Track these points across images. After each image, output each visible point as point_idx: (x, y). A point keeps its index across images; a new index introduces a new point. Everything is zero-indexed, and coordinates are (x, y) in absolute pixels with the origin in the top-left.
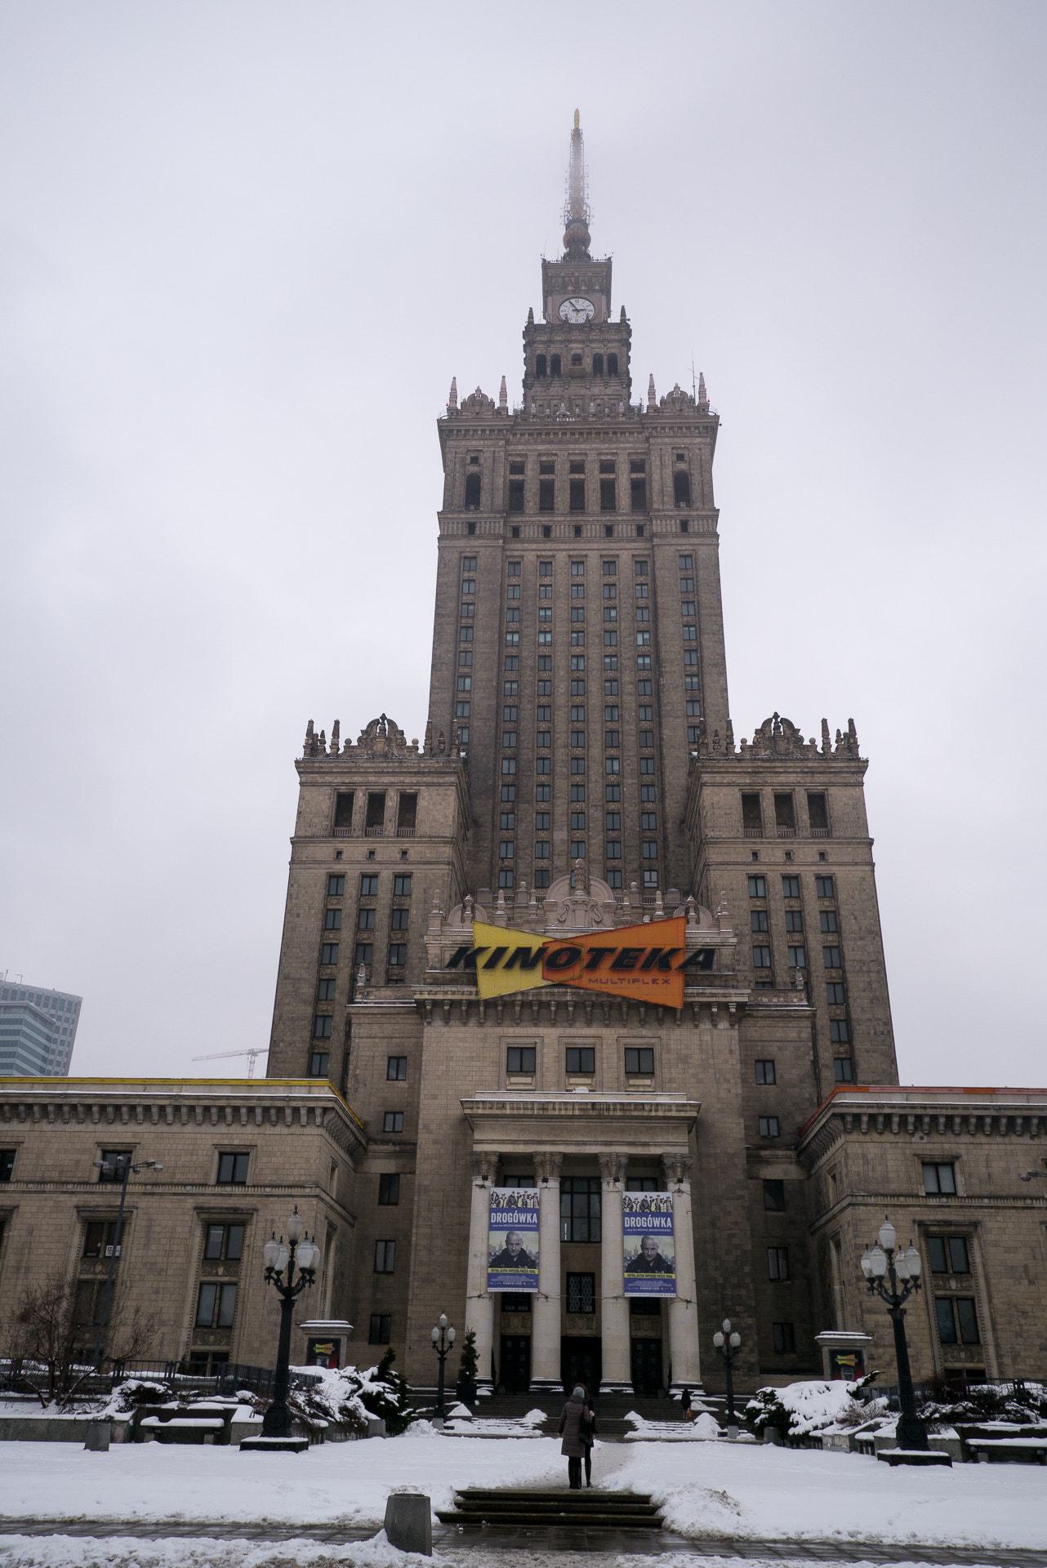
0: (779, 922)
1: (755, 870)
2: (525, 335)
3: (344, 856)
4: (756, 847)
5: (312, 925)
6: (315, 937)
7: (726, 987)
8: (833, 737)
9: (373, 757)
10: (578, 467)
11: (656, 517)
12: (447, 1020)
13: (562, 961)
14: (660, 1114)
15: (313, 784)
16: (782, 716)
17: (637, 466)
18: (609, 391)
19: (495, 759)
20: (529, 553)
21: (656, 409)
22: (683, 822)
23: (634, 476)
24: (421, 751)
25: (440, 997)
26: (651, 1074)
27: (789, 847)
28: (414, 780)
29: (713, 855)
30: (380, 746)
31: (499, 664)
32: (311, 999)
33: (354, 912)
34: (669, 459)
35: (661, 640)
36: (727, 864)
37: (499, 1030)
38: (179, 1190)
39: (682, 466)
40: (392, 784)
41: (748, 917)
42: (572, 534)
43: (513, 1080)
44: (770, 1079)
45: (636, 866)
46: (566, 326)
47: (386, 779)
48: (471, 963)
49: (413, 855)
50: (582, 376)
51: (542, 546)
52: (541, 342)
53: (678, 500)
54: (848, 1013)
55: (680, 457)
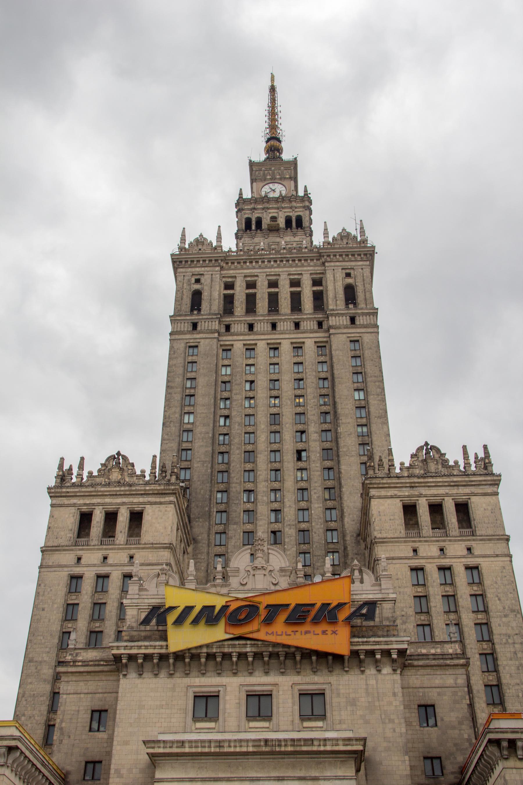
0: (437, 604)
1: (415, 563)
2: (237, 205)
3: (83, 561)
4: (416, 545)
6: (56, 627)
7: (388, 636)
8: (472, 460)
11: (332, 315)
13: (242, 617)
14: (328, 748)
15: (61, 506)
16: (431, 443)
17: (317, 282)
19: (211, 491)
21: (329, 243)
22: (358, 535)
23: (315, 288)
24: (147, 478)
25: (134, 651)
26: (323, 717)
27: (442, 544)
28: (141, 500)
30: (115, 476)
31: (214, 421)
32: (50, 678)
33: (89, 605)
35: (337, 400)
37: (187, 681)
39: (349, 281)
40: (124, 504)
41: (411, 601)
42: (270, 328)
44: (431, 722)
46: (266, 199)
51: (247, 337)
52: (248, 209)
53: (347, 304)
54: (499, 679)
55: (348, 275)
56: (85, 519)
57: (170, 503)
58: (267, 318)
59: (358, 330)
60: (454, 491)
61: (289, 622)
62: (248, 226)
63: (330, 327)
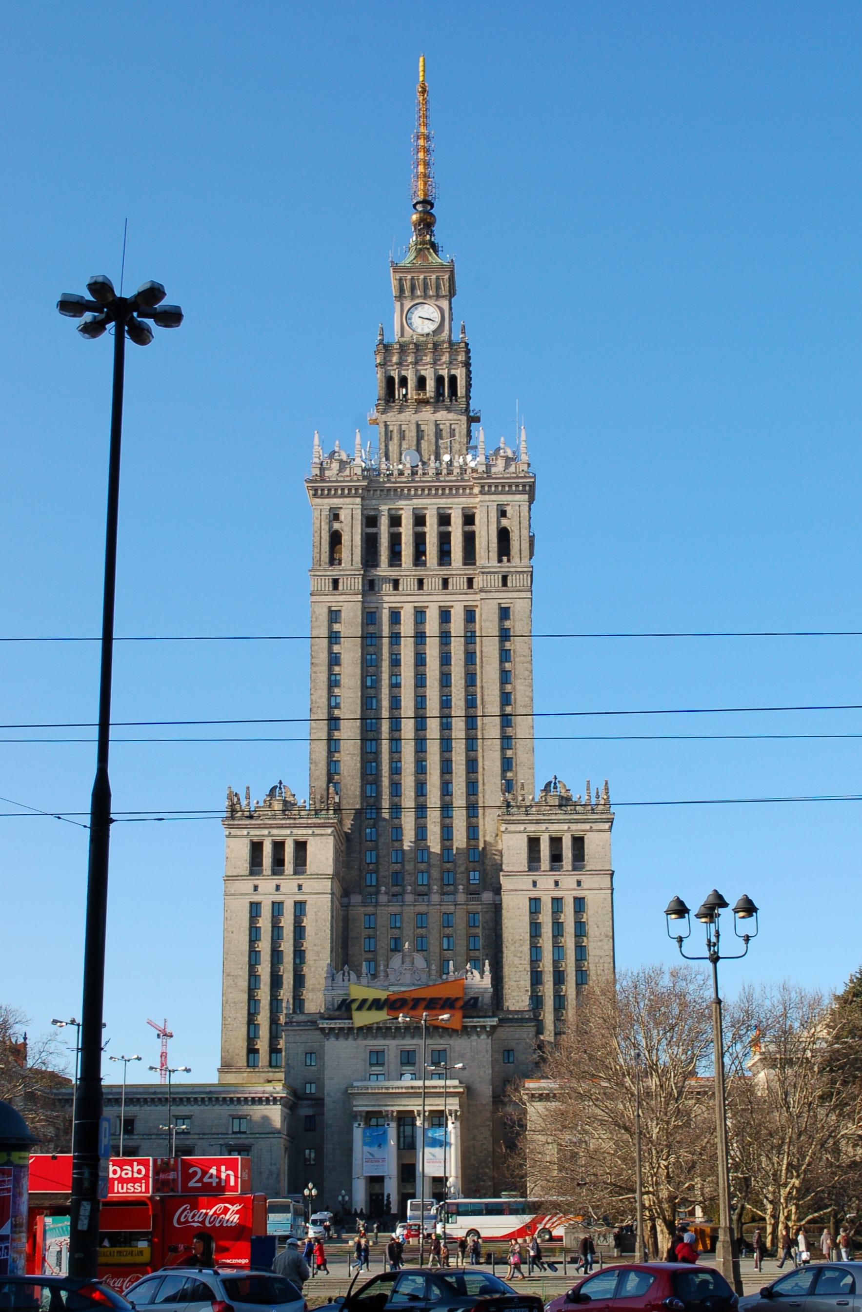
1: (534, 894)
3: (259, 889)
12: (337, 1037)
17: (469, 519)
27: (557, 878)
29: (506, 883)
32: (246, 989)
34: (493, 515)
35: (484, 685)
36: (516, 890)
37: (365, 1042)
38: (215, 1136)
43: (373, 1068)
44: (511, 1059)
49: (305, 888)
50: (426, 402)
57: (329, 835)
58: (413, 573)
59: (511, 595)
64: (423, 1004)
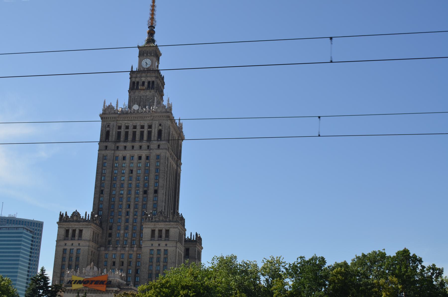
0: (155, 260)
1: (151, 248)
5: (60, 260)
6: (60, 263)
9: (73, 221)
10: (135, 127)
12: (67, 292)
17: (150, 127)
18: (151, 94)
20: (120, 154)
23: (149, 130)
27: (159, 243)
30: (75, 218)
33: (68, 258)
34: (157, 126)
39: (160, 128)
40: (77, 228)
41: (148, 259)
45: (138, 240)
47: (76, 226)
48: (71, 283)
51: (124, 152)
56: (67, 231)
60: (166, 226)
61: (95, 284)
62: (134, 87)
63: (151, 149)
64: (94, 282)
